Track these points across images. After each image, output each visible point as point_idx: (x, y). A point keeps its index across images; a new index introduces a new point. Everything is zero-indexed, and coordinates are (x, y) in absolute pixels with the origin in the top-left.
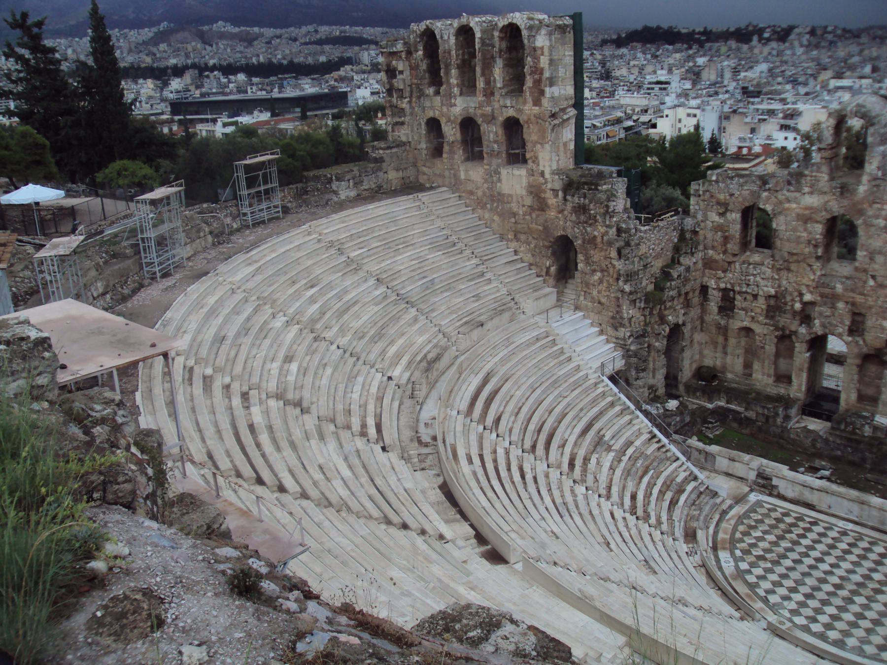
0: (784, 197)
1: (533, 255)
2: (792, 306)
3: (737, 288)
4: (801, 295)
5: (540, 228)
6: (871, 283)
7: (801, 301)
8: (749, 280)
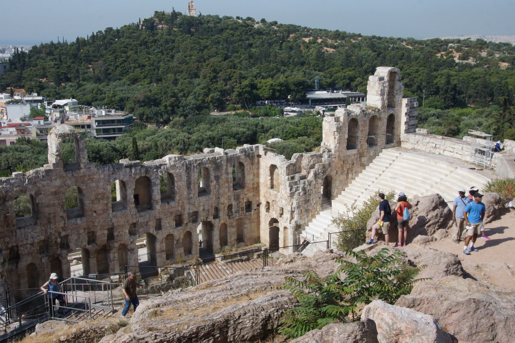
0: (40, 185)
2: (56, 242)
3: (20, 244)
4: (60, 233)
6: (95, 214)
7: (60, 236)
8: (28, 236)
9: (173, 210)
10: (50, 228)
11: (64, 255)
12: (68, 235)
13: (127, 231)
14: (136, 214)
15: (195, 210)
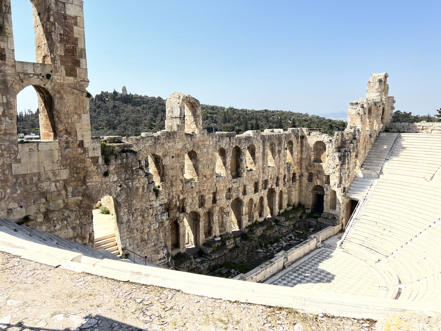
0: (167, 146)
1: (74, 228)
5: (80, 198)
6: (205, 179)
7: (179, 199)
9: (254, 177)
10: (172, 190)
11: (182, 218)
12: (185, 198)
13: (225, 195)
14: (231, 180)
15: (266, 178)
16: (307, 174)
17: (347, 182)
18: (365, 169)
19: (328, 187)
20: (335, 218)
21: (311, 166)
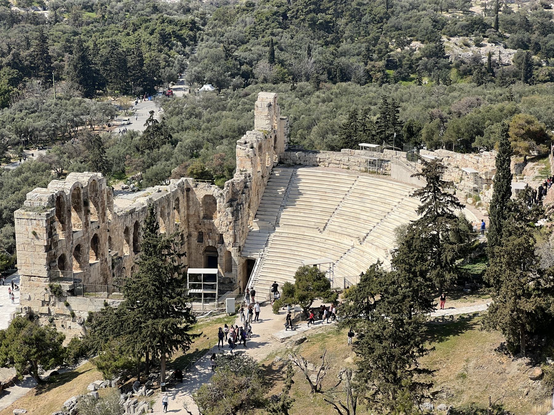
16: (196, 233)
17: (242, 239)
18: (262, 220)
19: (222, 247)
20: (232, 282)
21: (200, 224)
